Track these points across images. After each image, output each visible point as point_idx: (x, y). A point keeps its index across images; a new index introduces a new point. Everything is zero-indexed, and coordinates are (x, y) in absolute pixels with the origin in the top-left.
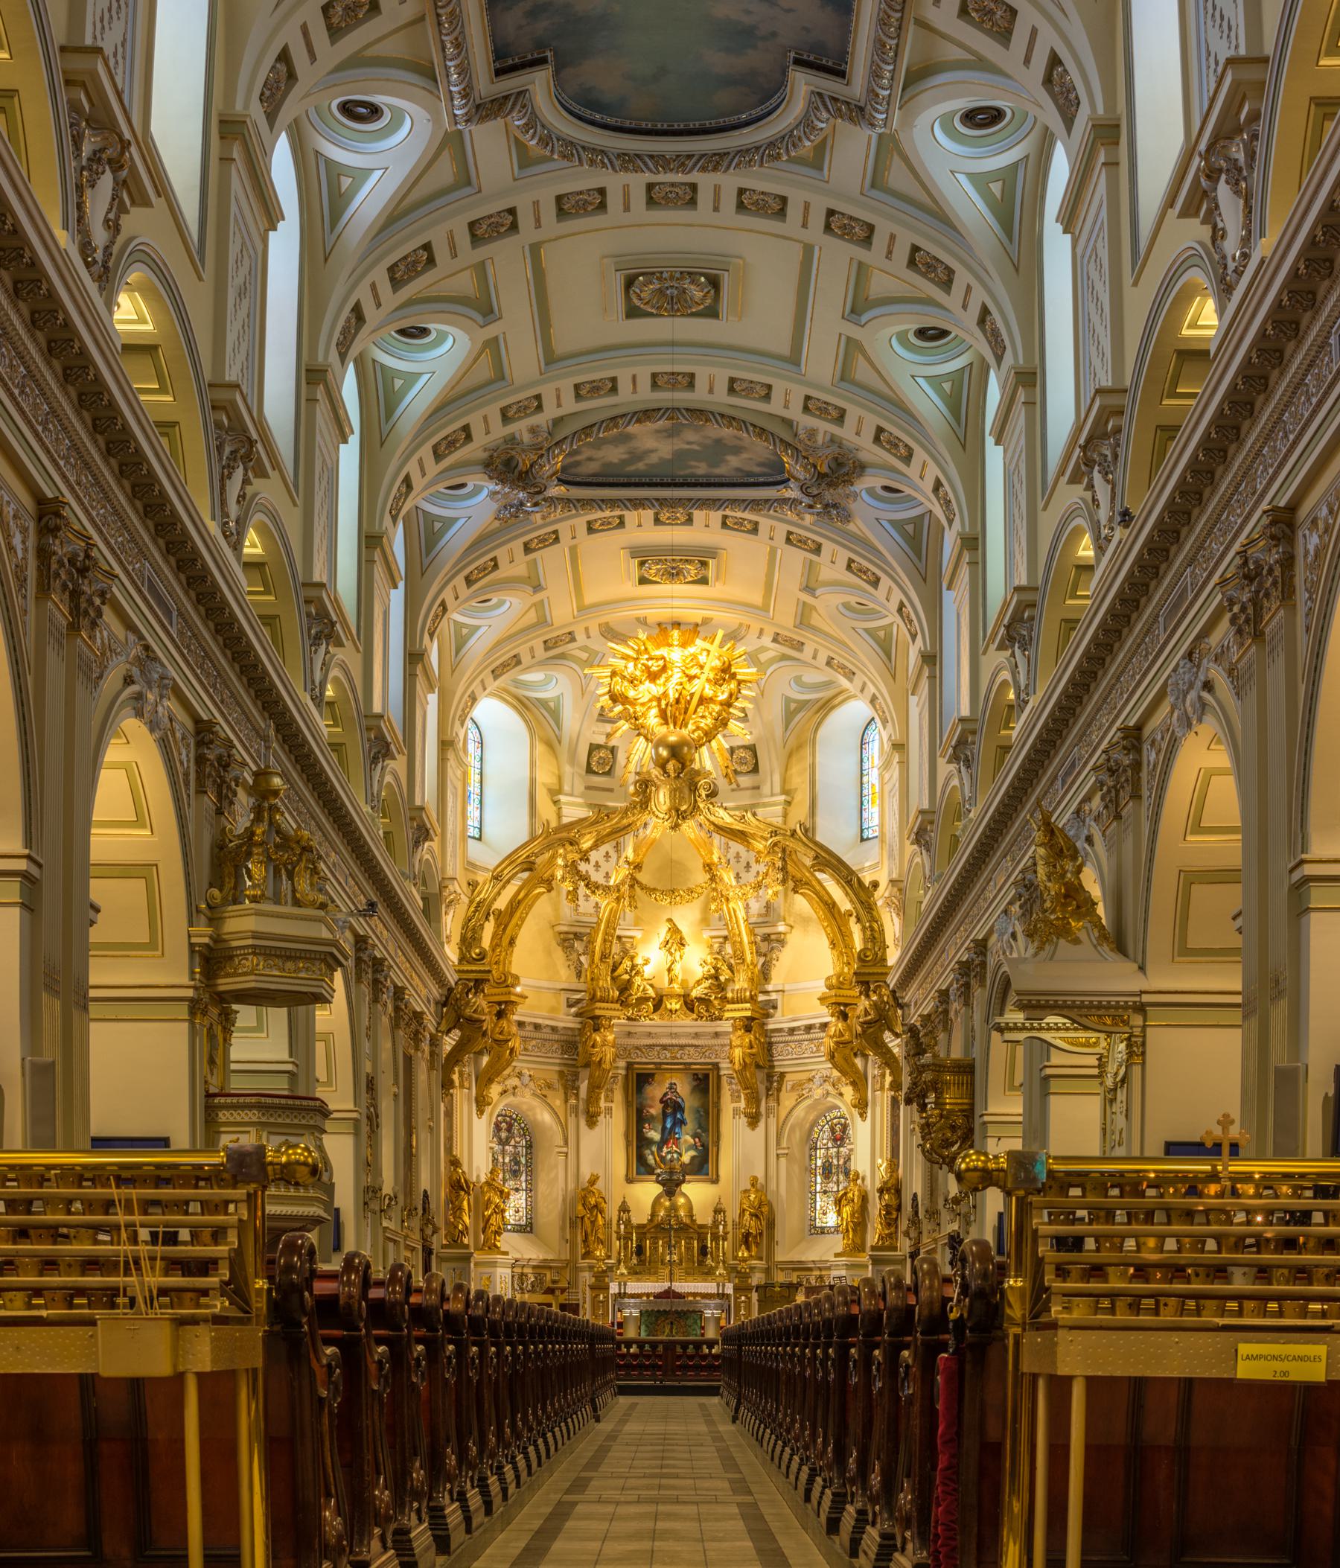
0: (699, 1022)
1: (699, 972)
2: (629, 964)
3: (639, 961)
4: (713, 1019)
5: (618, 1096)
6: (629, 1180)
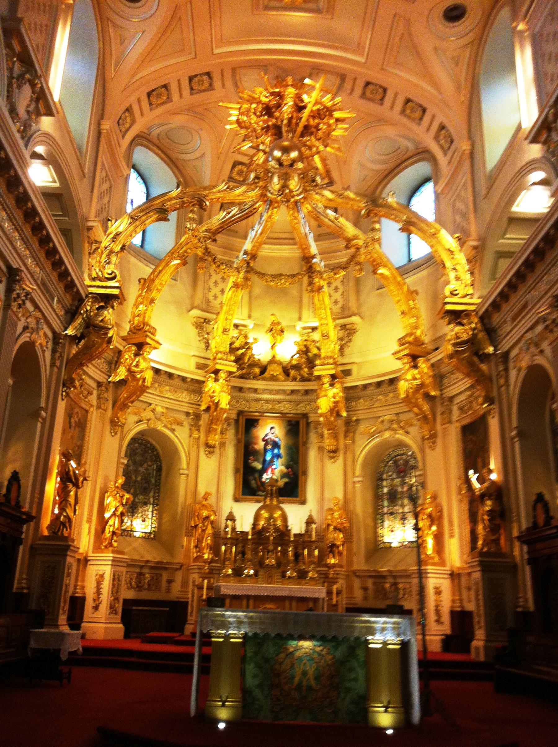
0: (294, 383)
1: (295, 349)
2: (244, 340)
3: (250, 340)
4: (303, 379)
5: (231, 434)
6: (237, 500)
